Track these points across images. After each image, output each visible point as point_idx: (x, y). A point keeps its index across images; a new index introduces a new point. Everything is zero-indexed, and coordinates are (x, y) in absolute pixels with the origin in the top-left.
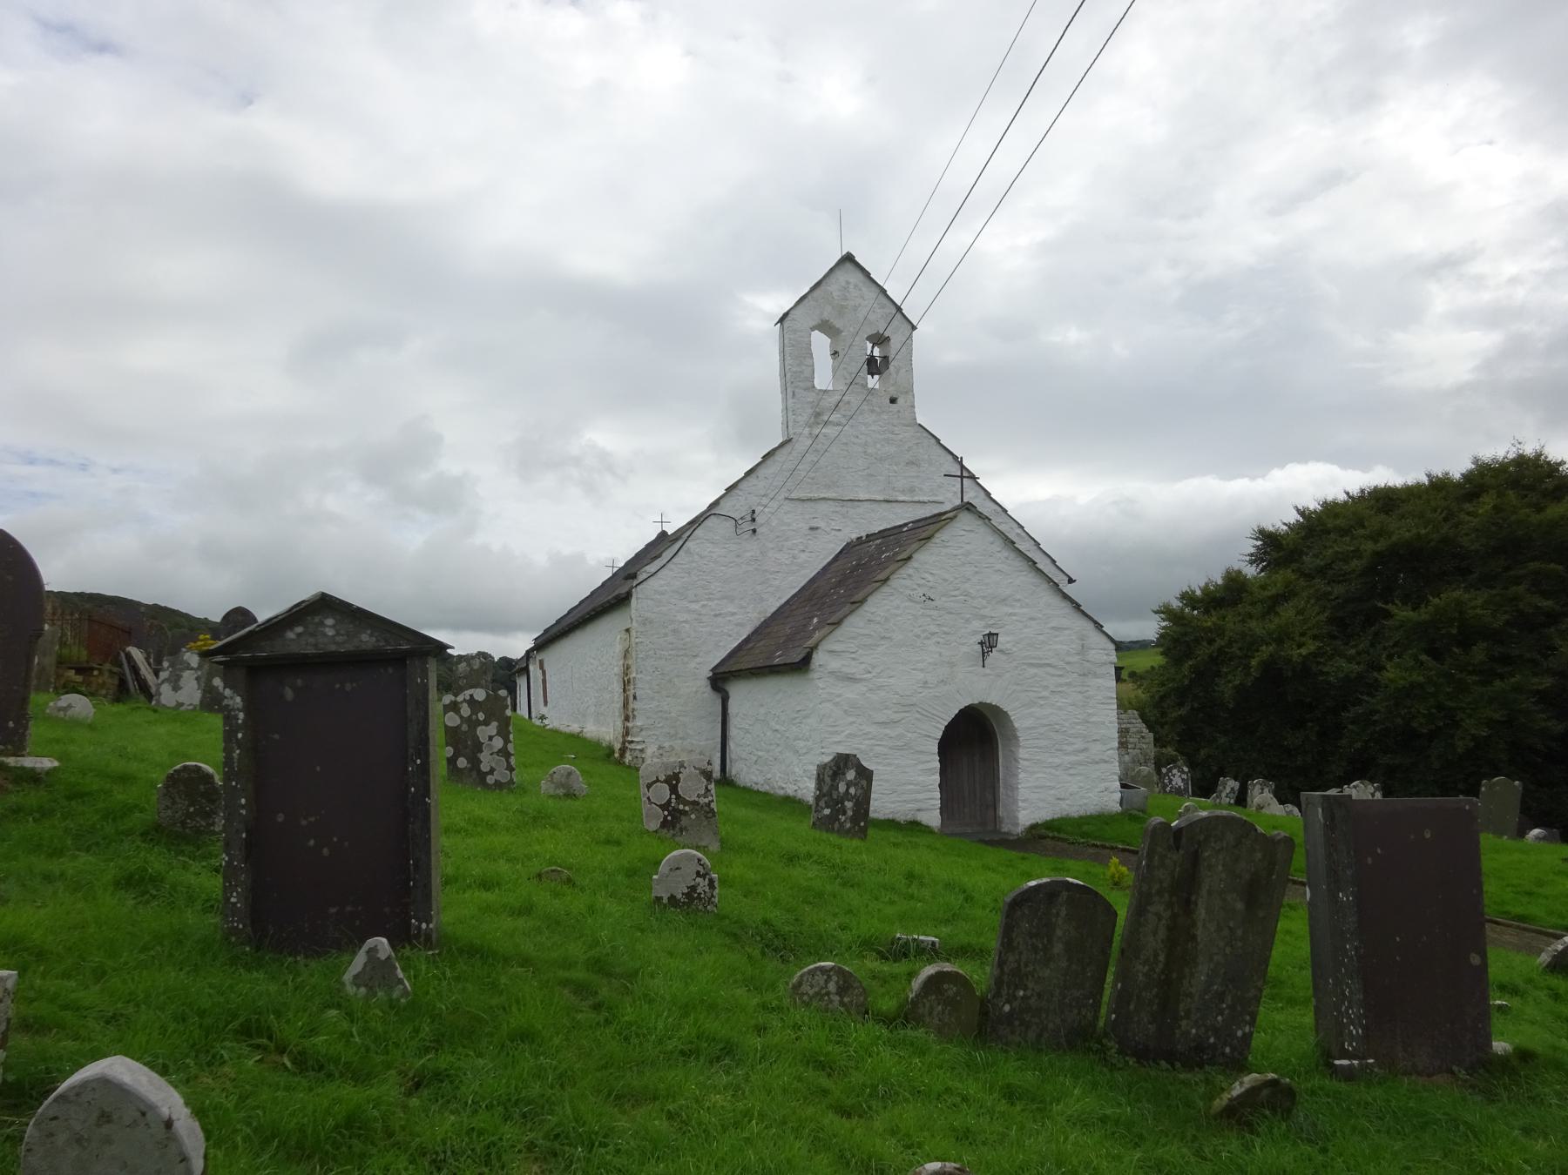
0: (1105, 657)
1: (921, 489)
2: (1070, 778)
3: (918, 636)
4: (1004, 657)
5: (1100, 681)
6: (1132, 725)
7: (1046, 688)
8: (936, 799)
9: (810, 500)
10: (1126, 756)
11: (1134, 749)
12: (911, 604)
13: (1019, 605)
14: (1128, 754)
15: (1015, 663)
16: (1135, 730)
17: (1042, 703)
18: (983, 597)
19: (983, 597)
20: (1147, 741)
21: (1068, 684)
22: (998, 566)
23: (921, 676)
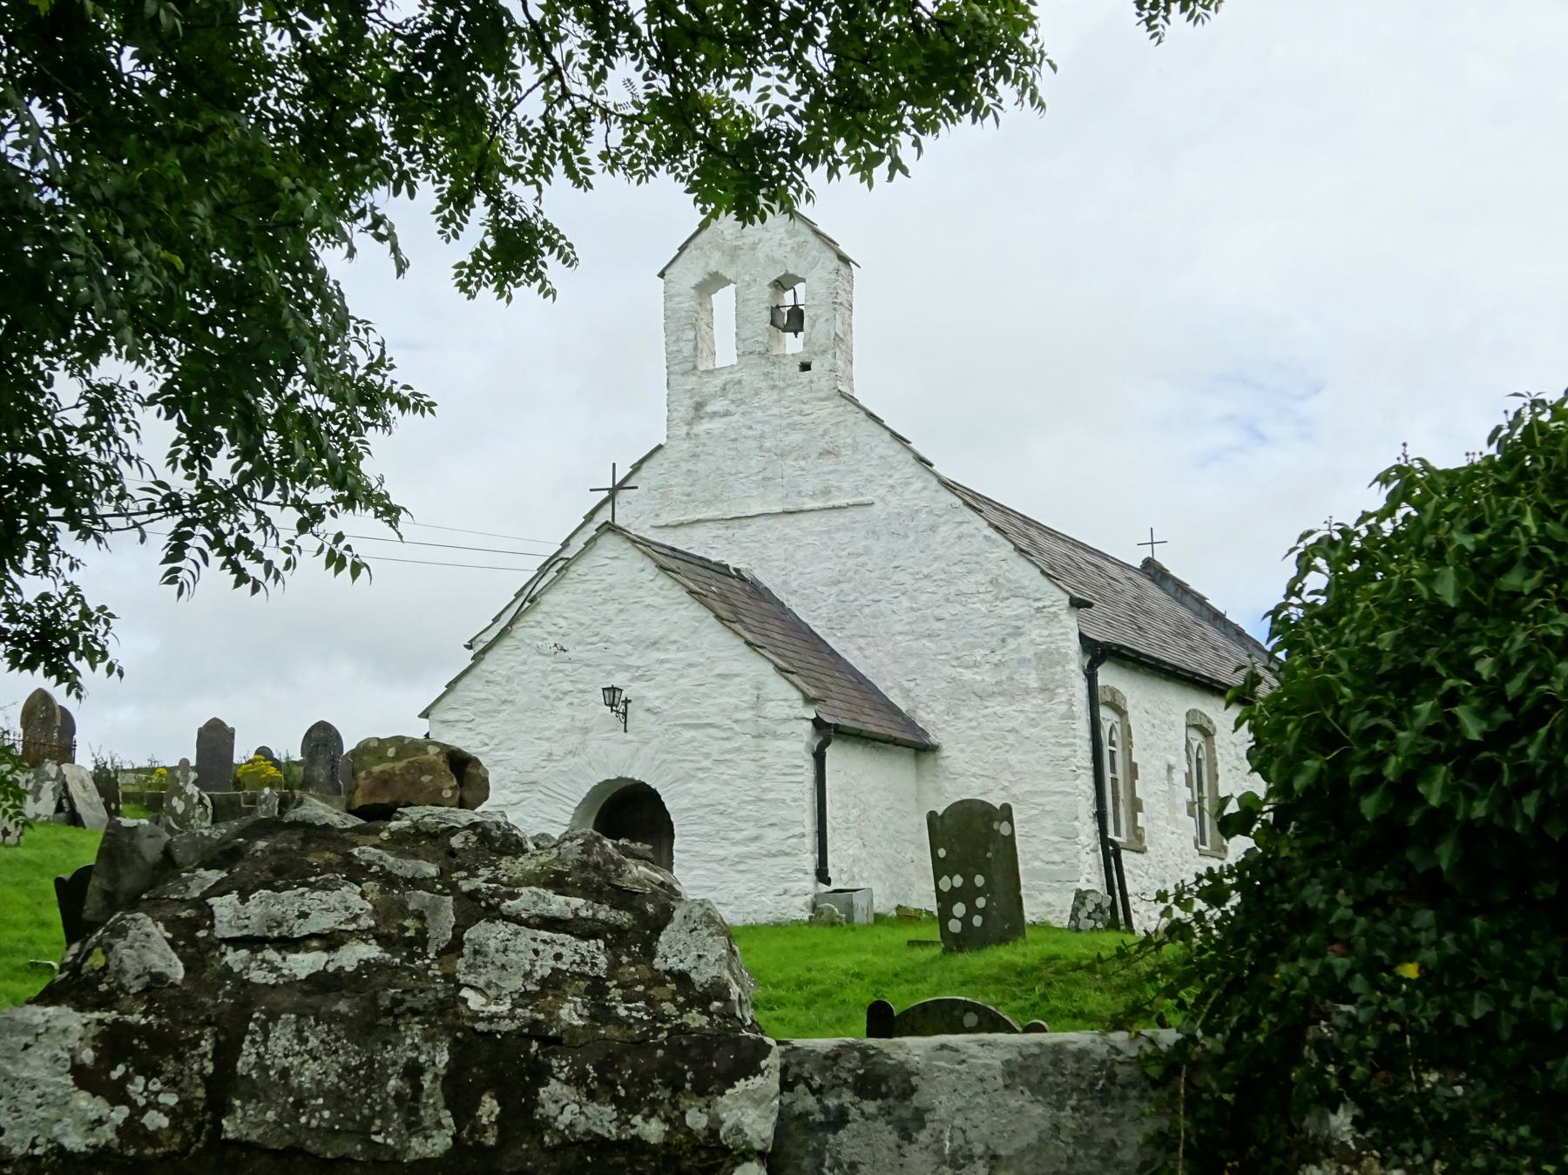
0: (788, 711)
1: (839, 489)
2: (738, 876)
3: (547, 697)
4: (653, 718)
5: (781, 743)
7: (707, 756)
8: (932, 943)
9: (681, 525)
12: (540, 658)
13: (674, 647)
15: (665, 725)
17: (701, 775)
18: (628, 642)
19: (628, 642)
21: (738, 750)
22: (649, 600)
23: (546, 746)
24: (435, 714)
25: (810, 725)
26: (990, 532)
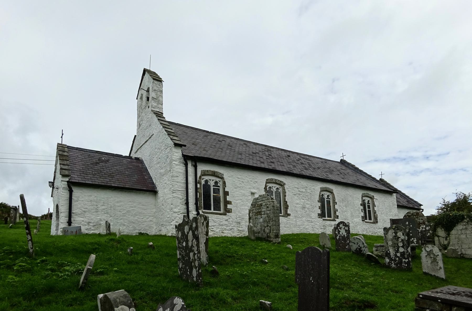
6: (263, 202)
10: (261, 219)
11: (264, 214)
14: (262, 218)
16: (264, 204)
20: (269, 209)
24: (53, 196)
25: (66, 183)
26: (165, 132)
